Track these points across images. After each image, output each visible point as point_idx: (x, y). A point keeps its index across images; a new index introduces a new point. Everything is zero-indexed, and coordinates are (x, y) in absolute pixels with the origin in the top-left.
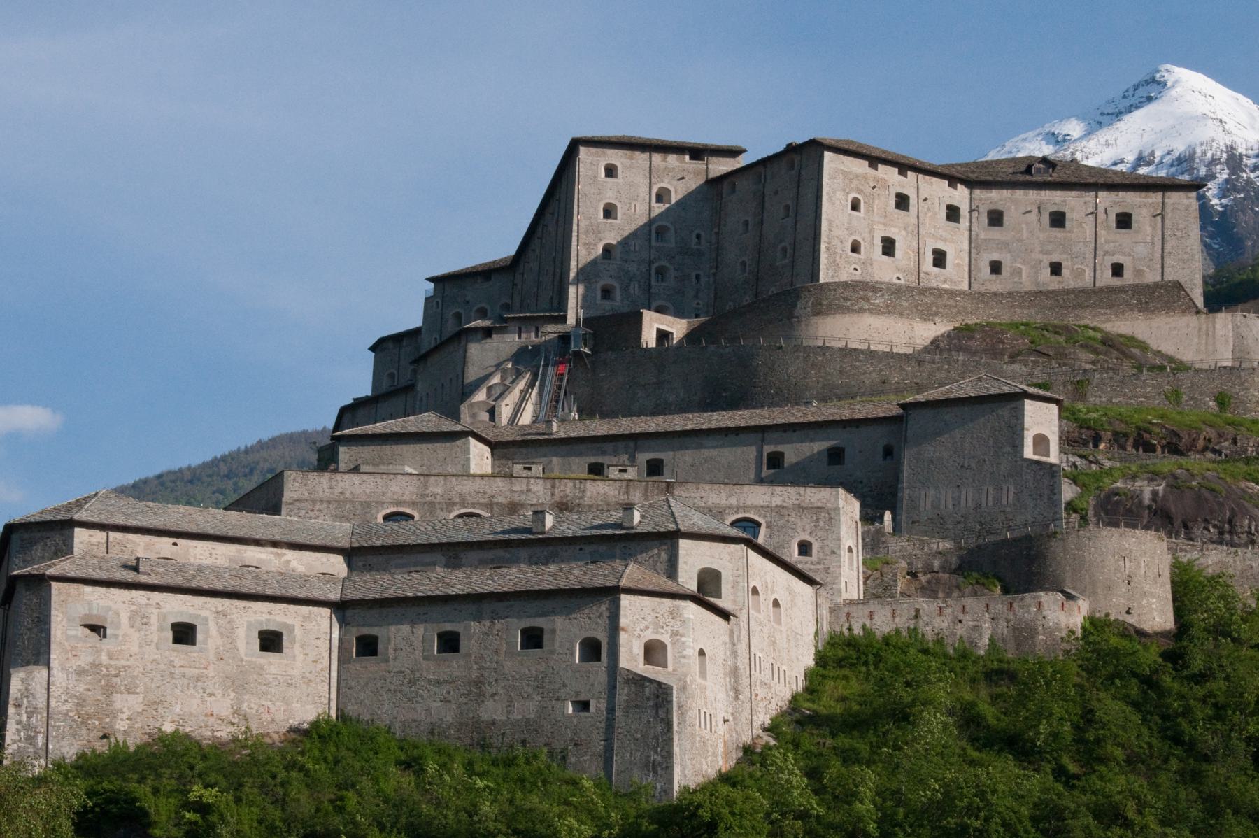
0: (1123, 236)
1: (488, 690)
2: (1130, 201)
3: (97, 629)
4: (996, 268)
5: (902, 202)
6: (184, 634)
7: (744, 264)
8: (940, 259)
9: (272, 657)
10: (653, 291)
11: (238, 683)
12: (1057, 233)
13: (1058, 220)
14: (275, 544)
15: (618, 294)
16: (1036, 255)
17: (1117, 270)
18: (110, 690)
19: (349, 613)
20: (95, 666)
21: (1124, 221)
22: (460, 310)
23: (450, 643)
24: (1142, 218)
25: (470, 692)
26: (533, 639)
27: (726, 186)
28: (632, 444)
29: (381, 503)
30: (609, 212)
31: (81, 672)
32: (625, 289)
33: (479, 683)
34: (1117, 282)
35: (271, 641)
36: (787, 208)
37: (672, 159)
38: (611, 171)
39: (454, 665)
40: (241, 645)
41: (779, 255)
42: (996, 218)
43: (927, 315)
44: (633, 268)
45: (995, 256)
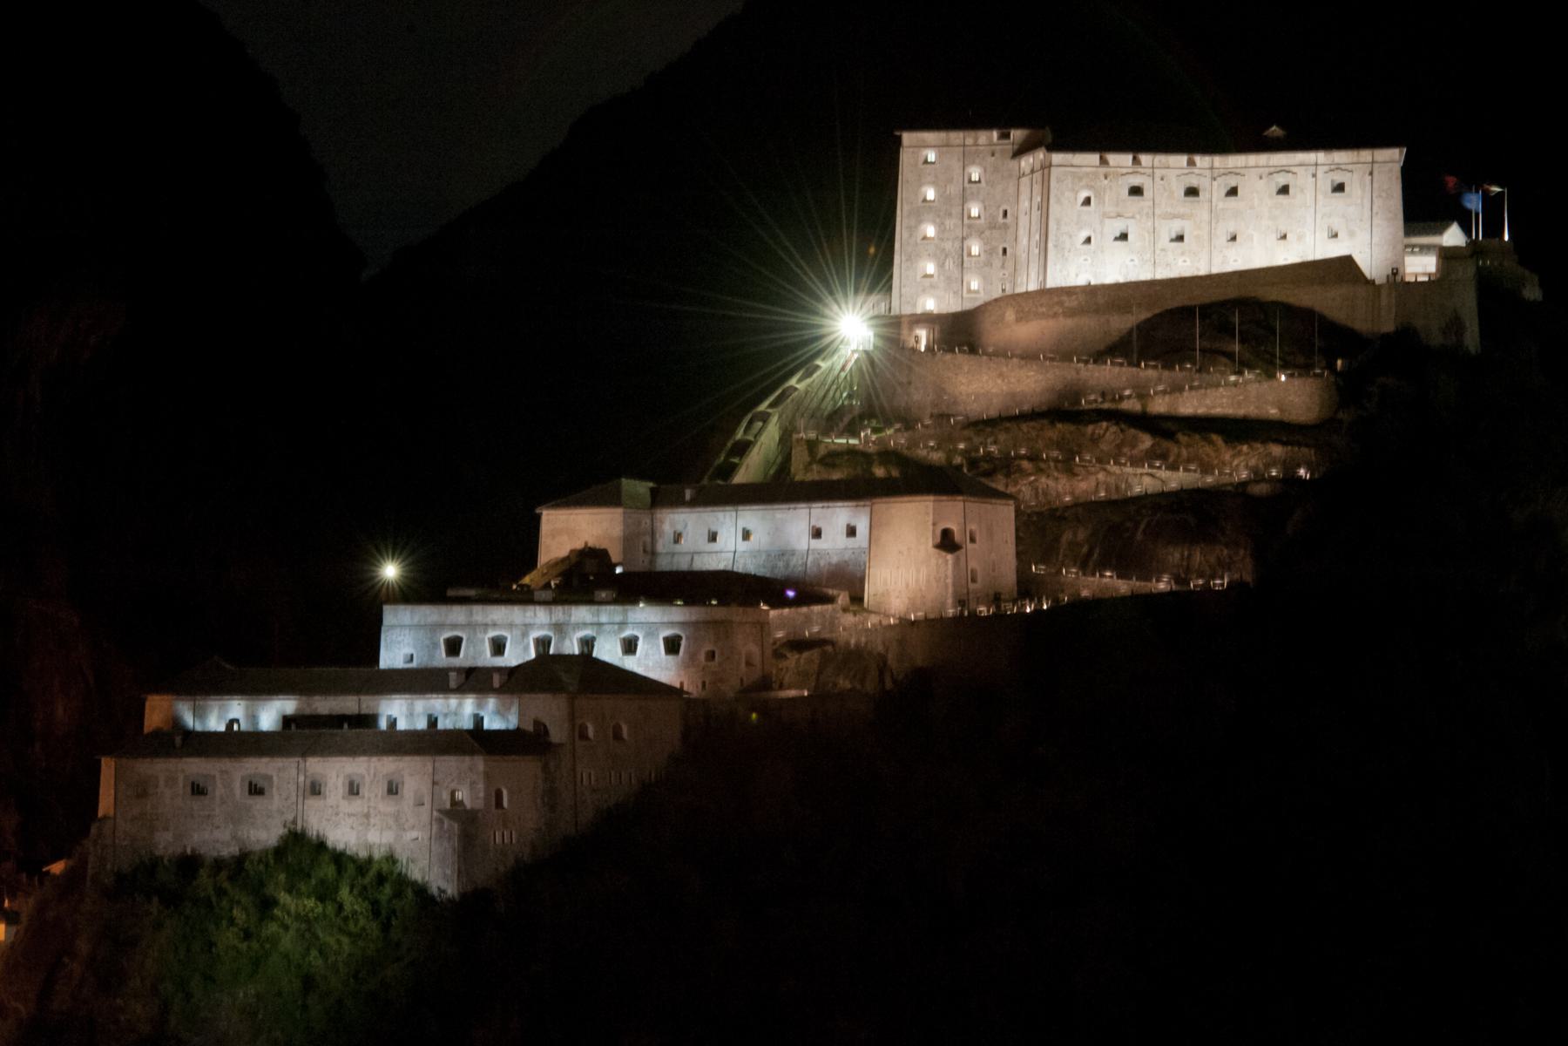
10: (965, 265)
33: (367, 816)
40: (238, 792)
44: (948, 245)
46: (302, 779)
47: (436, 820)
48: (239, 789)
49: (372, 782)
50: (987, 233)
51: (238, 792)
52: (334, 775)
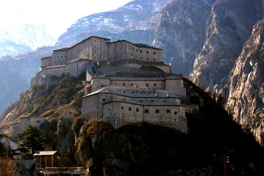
0: (154, 55)
1: (163, 117)
2: (155, 51)
6: (130, 109)
7: (113, 55)
8: (136, 56)
9: (138, 112)
11: (135, 115)
12: (148, 54)
13: (148, 53)
14: (126, 96)
15: (97, 57)
16: (146, 57)
17: (154, 59)
18: (124, 116)
19: (144, 107)
20: (123, 113)
21: (155, 53)
22: (58, 56)
23: (157, 111)
24: (157, 53)
25: (161, 118)
26: (168, 111)
27: (110, 45)
28: (129, 81)
29: (122, 90)
30: (95, 47)
31: (122, 114)
32: (98, 57)
33: (162, 116)
34: (154, 61)
35: (137, 110)
36: (120, 48)
37: (102, 40)
38: (95, 41)
39: (158, 114)
40: (135, 110)
41: (119, 54)
43: (140, 64)
44: (99, 54)
45: (141, 56)
46: (143, 109)
47: (181, 117)
48: (135, 110)
49: (162, 110)
50: (104, 53)
51: (135, 110)
52: (152, 110)
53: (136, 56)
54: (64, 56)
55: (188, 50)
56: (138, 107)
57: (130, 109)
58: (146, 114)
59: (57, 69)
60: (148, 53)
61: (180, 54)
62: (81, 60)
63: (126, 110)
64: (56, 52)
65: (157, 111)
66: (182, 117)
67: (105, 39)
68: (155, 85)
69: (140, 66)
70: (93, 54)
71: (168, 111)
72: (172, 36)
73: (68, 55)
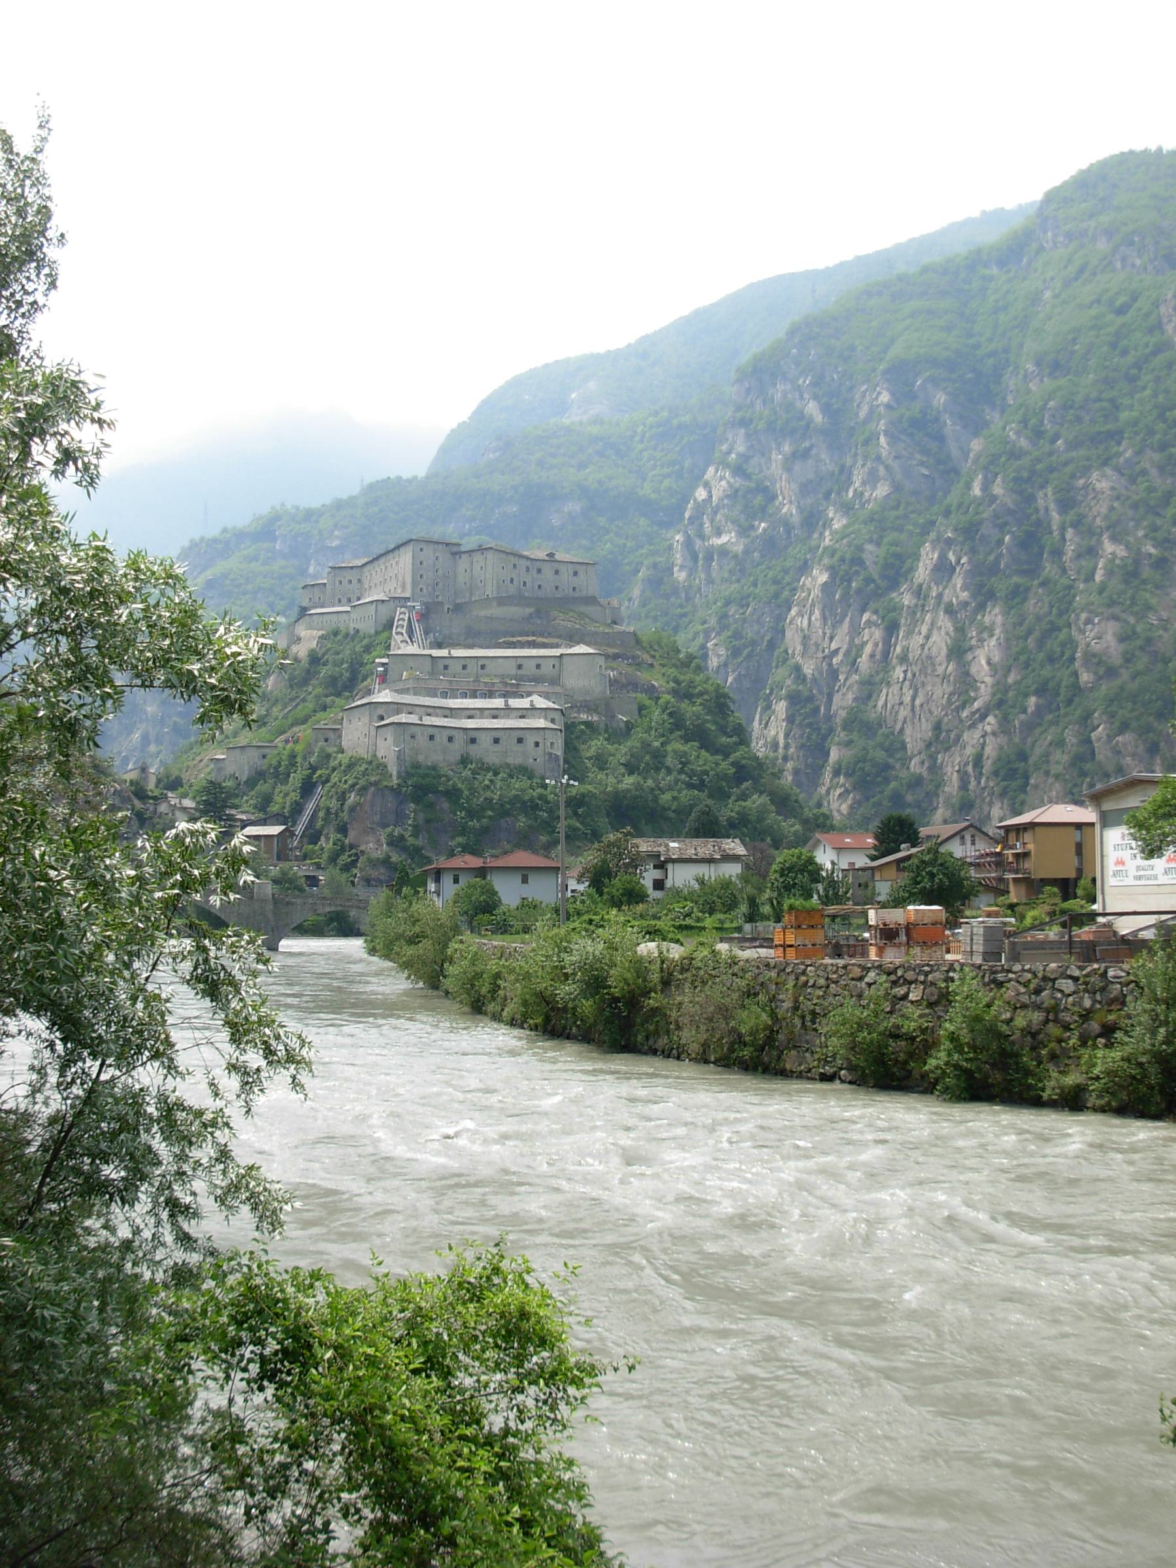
2: (578, 567)
3: (413, 737)
4: (540, 587)
5: (515, 566)
6: (432, 738)
8: (525, 583)
13: (557, 572)
21: (575, 574)
23: (496, 741)
26: (520, 741)
35: (450, 739)
39: (497, 748)
42: (539, 571)
48: (445, 739)
53: (525, 583)
54: (355, 582)
55: (809, 501)
56: (453, 733)
57: (432, 738)
58: (472, 747)
59: (334, 617)
60: (557, 572)
61: (784, 510)
62: (386, 599)
63: (422, 740)
64: (337, 571)
65: (496, 741)
66: (550, 754)
67: (447, 544)
68: (538, 666)
69: (529, 610)
70: (415, 583)
71: (520, 741)
72: (763, 455)
73: (364, 579)
